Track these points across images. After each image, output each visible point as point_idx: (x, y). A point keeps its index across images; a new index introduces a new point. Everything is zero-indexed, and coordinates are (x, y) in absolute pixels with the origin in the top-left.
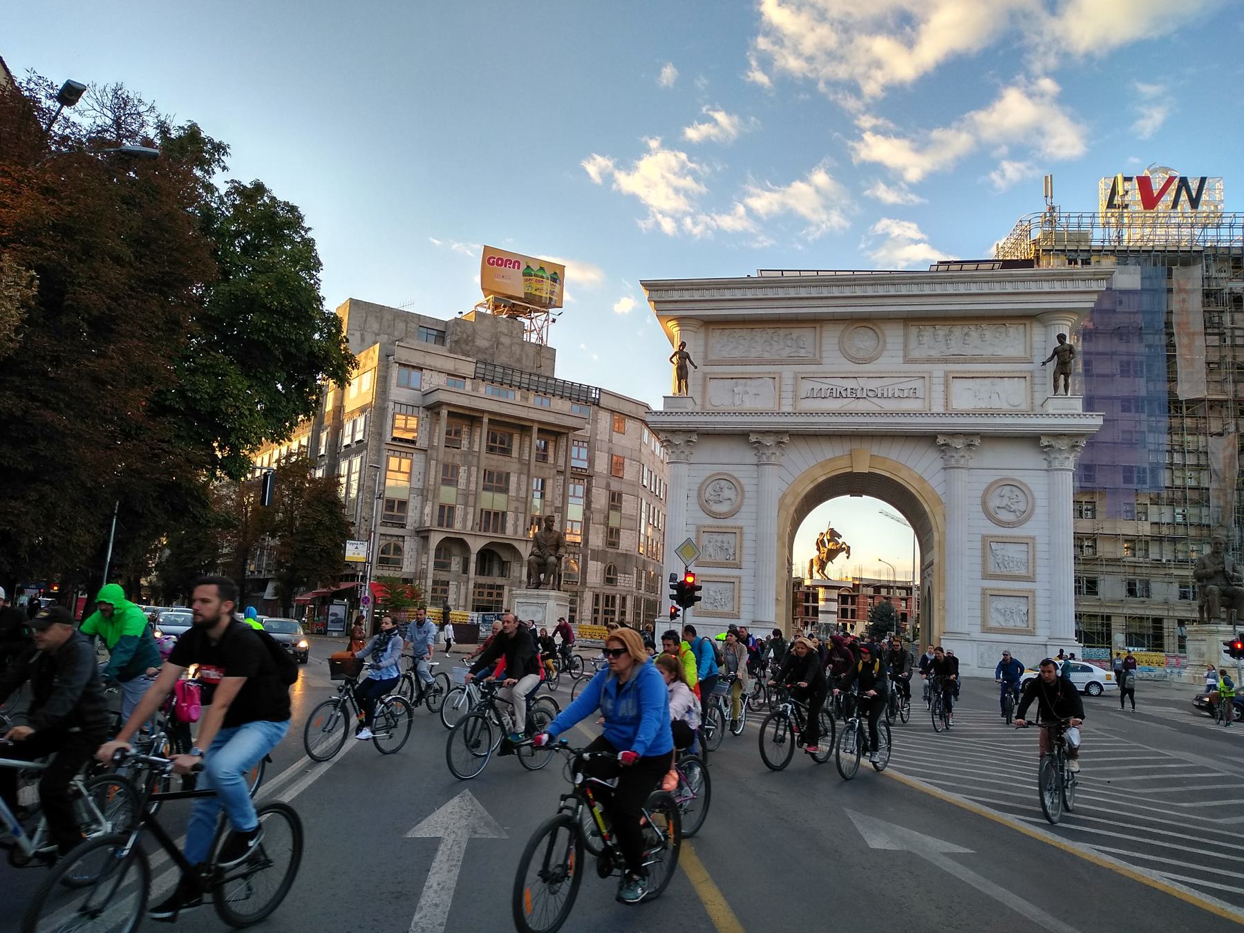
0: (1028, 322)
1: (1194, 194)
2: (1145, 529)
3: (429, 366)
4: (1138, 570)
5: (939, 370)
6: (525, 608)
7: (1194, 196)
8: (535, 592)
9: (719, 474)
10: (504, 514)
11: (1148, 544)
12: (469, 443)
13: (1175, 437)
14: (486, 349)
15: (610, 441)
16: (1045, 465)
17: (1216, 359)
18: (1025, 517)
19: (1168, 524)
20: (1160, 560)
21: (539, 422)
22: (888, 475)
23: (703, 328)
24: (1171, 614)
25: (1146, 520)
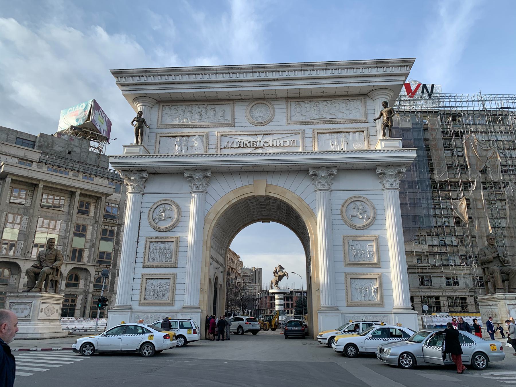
0: (362, 98)
1: (430, 91)
2: (426, 248)
3: (5, 152)
4: (425, 271)
5: (309, 129)
6: (16, 306)
9: (163, 200)
11: (428, 257)
13: (435, 201)
14: (61, 152)
16: (381, 187)
17: (450, 162)
19: (437, 246)
20: (435, 265)
21: (81, 189)
23: (157, 106)
24: (444, 294)
25: (426, 244)
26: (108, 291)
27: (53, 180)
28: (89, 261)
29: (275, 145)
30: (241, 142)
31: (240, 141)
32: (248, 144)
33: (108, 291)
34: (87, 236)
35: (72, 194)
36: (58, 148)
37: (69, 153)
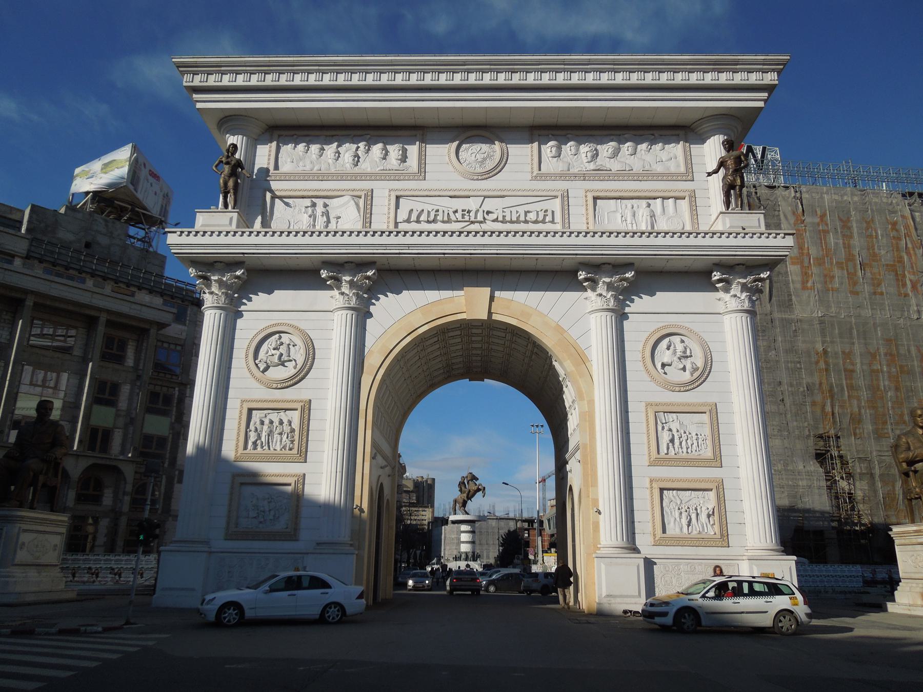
1: (759, 156)
18: (702, 376)
21: (109, 312)
22: (514, 322)
28: (123, 451)
29: (508, 218)
30: (438, 211)
31: (436, 208)
32: (452, 215)
34: (120, 404)
35: (90, 322)
36: (65, 235)
37: (88, 245)
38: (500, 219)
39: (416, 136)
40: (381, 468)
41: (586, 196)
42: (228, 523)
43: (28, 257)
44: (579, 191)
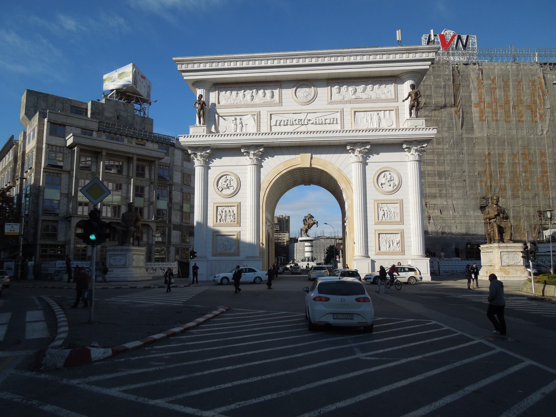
1: (465, 41)
3: (70, 124)
7: (464, 44)
8: (120, 248)
10: (119, 206)
12: (97, 167)
15: (182, 166)
18: (398, 188)
21: (137, 154)
26: (167, 243)
27: (114, 148)
28: (149, 217)
29: (318, 123)
30: (288, 120)
32: (294, 121)
33: (167, 243)
35: (129, 159)
37: (118, 118)
38: (314, 123)
39: (277, 85)
40: (268, 226)
41: (351, 111)
42: (213, 250)
43: (99, 131)
44: (348, 108)
